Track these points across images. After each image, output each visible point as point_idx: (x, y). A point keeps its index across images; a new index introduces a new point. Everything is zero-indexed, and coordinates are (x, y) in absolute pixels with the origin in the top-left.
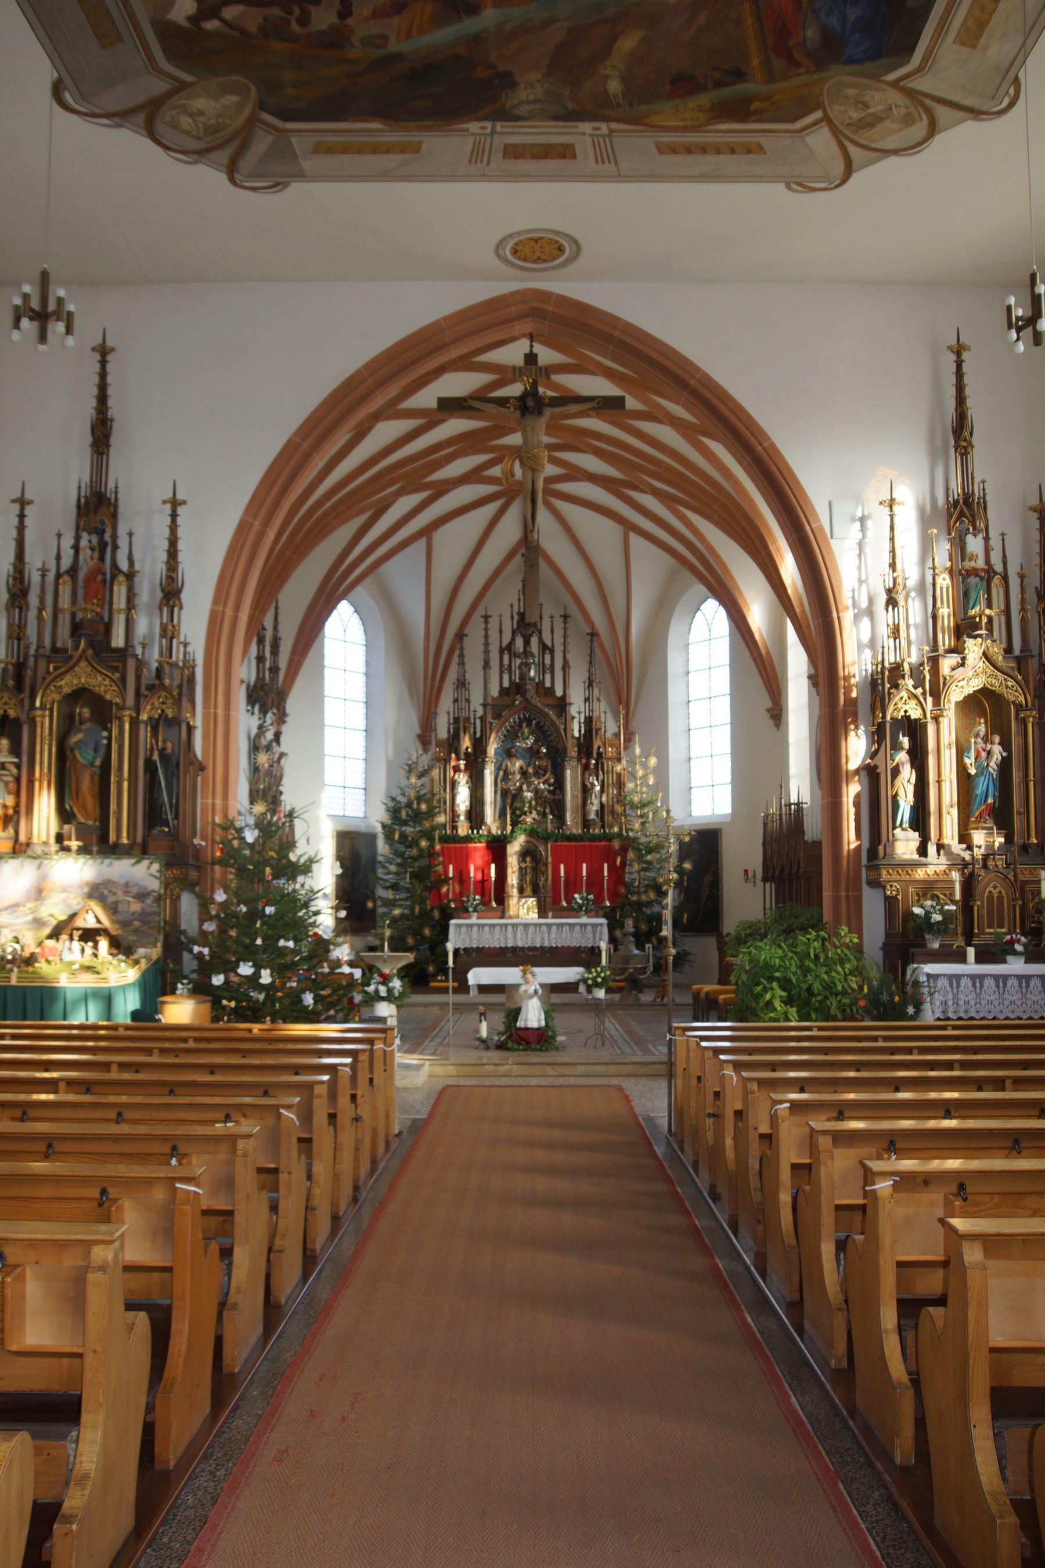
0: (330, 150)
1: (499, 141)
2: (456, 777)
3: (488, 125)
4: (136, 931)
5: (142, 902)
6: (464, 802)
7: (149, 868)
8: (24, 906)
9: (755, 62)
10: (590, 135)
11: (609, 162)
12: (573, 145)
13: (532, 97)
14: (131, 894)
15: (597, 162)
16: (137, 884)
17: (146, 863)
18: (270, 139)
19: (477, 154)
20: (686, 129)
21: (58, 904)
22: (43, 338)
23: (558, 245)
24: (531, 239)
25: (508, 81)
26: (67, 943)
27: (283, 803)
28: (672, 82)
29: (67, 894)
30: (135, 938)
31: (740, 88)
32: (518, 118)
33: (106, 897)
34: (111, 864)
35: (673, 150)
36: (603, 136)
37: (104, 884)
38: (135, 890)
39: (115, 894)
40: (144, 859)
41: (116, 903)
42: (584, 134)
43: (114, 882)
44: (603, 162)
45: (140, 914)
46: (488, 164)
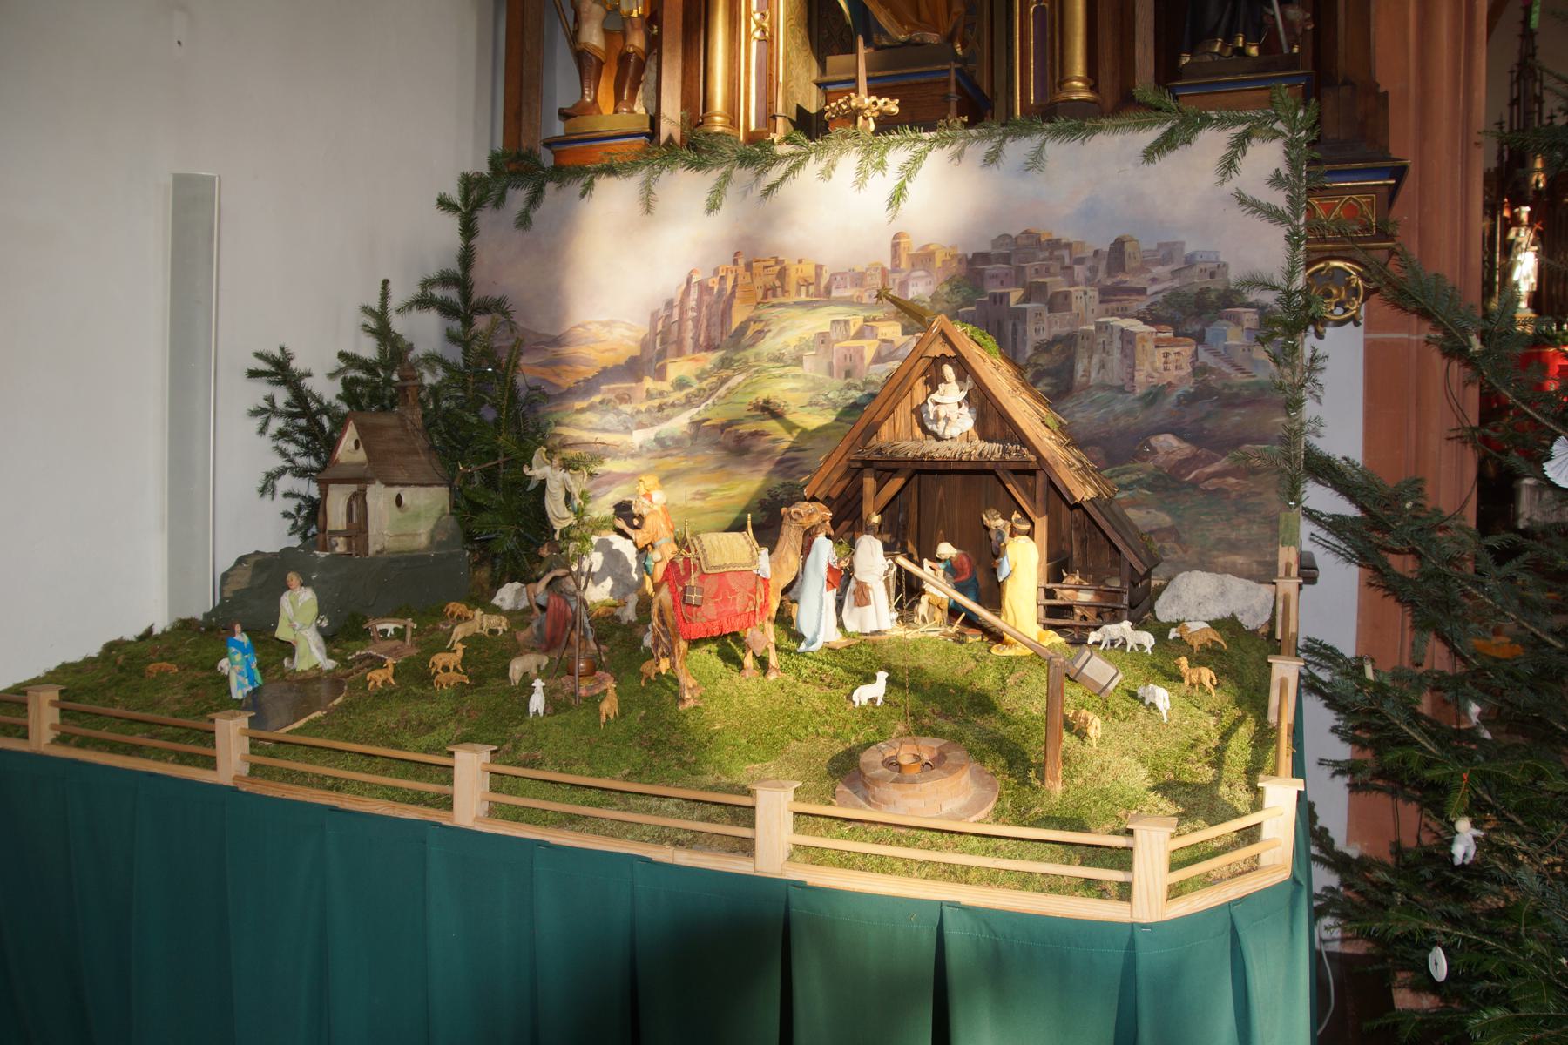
2: (1512, 235)
4: (1168, 483)
5: (1200, 339)
6: (1528, 277)
7: (1229, 165)
8: (660, 374)
14: (1141, 304)
16: (1167, 253)
17: (1212, 142)
21: (798, 361)
26: (824, 550)
29: (840, 313)
30: (1164, 519)
33: (1019, 315)
34: (1036, 161)
37: (1006, 259)
38: (1159, 282)
39: (1059, 302)
40: (1206, 121)
41: (1067, 344)
43: (1055, 244)
45: (1190, 399)
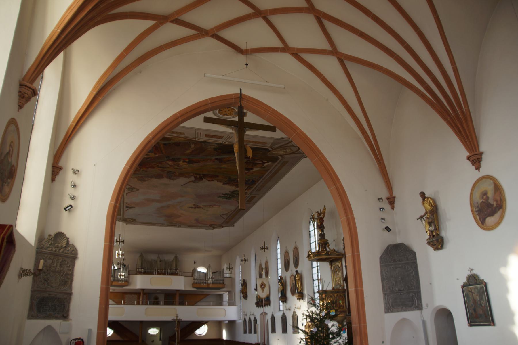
0: (264, 143)
1: (223, 140)
3: (223, 143)
9: (162, 146)
10: (200, 138)
11: (197, 133)
12: (205, 137)
13: (211, 146)
15: (200, 133)
18: (274, 146)
19: (230, 138)
20: (177, 137)
22: (265, 251)
23: (220, 112)
24: (227, 115)
25: (215, 149)
28: (180, 145)
31: (165, 142)
32: (216, 143)
35: (180, 133)
36: (197, 138)
42: (202, 139)
44: (199, 133)
46: (228, 136)
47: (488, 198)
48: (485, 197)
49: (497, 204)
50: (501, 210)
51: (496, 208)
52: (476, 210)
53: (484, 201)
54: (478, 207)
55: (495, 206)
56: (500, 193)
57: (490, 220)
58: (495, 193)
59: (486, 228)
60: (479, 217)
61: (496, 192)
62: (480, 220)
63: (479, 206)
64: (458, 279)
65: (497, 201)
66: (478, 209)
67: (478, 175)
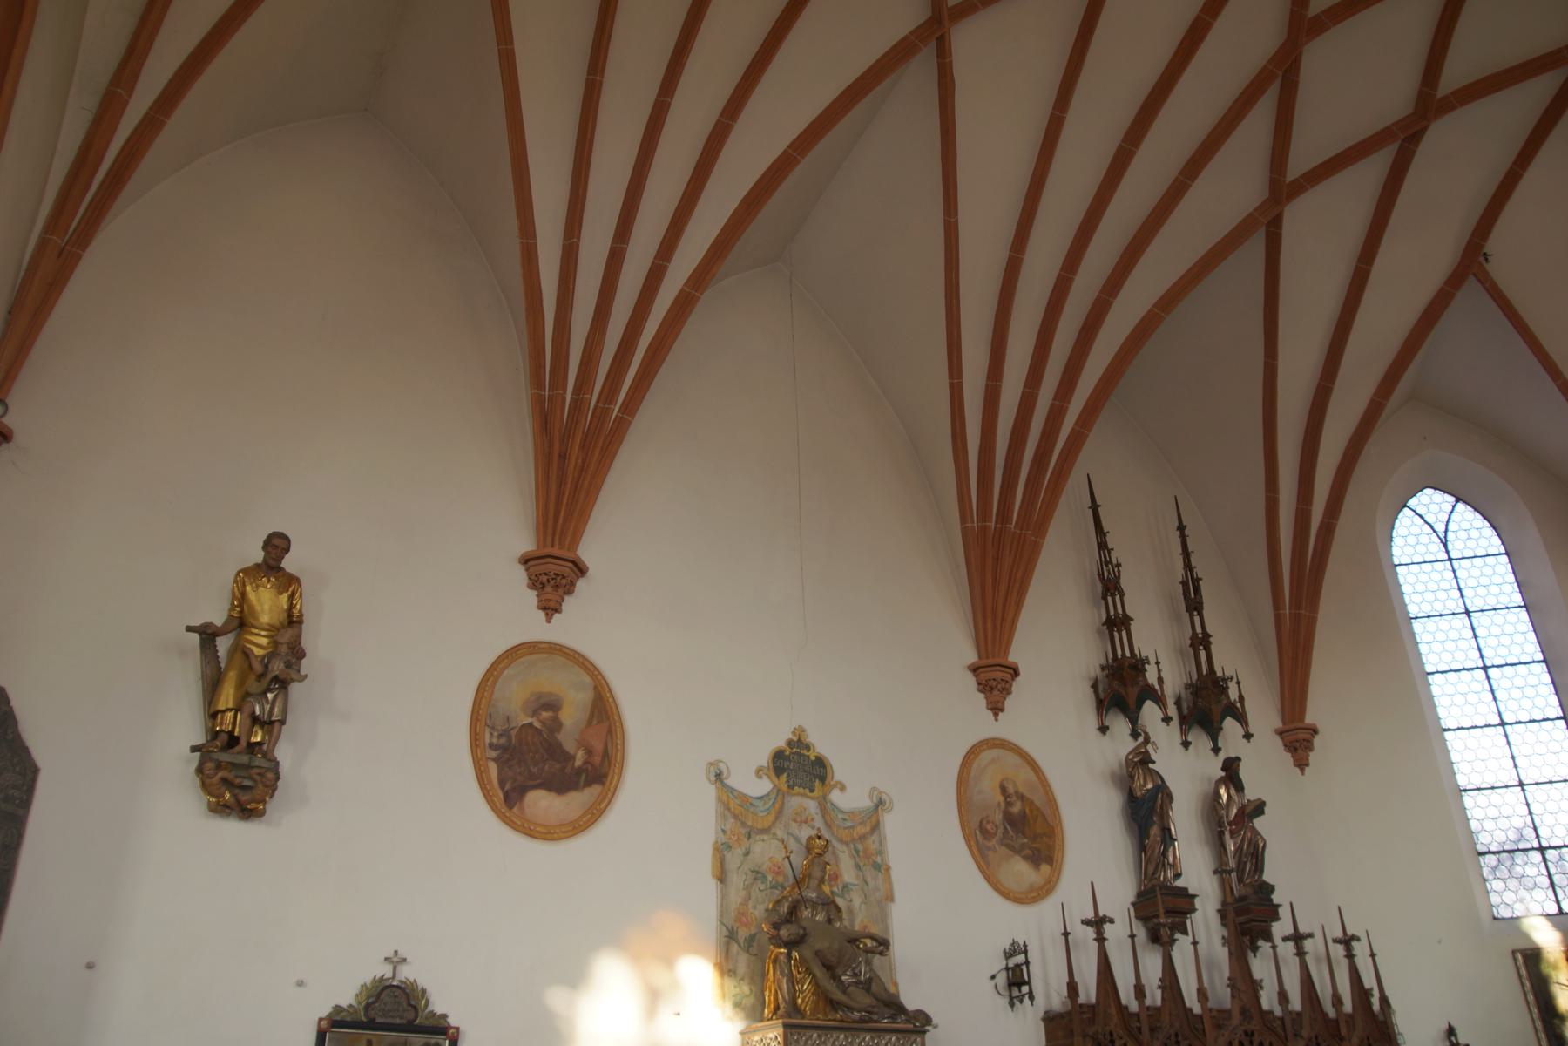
27: (1284, 912)
47: (556, 725)
48: (545, 714)
49: (585, 763)
50: (595, 789)
51: (579, 771)
52: (495, 741)
53: (537, 724)
54: (504, 734)
55: (578, 763)
56: (610, 732)
57: (541, 802)
58: (589, 723)
59: (519, 823)
60: (499, 773)
61: (595, 722)
62: (502, 783)
63: (514, 733)
64: (300, 984)
65: (589, 752)
66: (503, 740)
67: (534, 626)
